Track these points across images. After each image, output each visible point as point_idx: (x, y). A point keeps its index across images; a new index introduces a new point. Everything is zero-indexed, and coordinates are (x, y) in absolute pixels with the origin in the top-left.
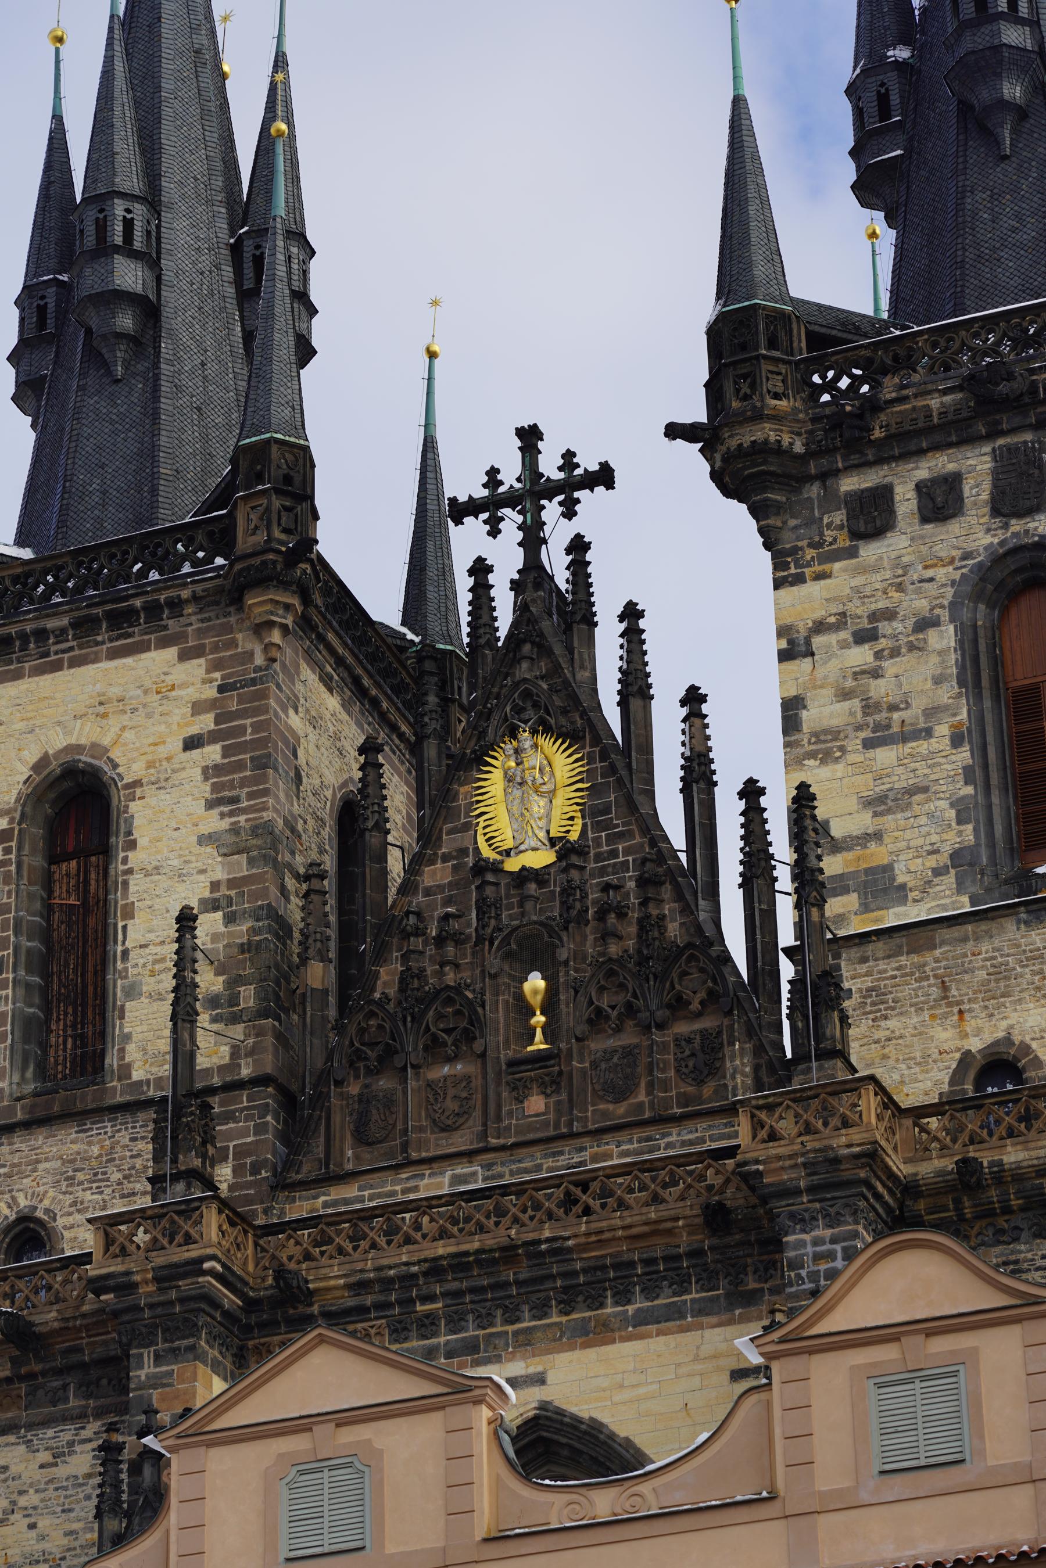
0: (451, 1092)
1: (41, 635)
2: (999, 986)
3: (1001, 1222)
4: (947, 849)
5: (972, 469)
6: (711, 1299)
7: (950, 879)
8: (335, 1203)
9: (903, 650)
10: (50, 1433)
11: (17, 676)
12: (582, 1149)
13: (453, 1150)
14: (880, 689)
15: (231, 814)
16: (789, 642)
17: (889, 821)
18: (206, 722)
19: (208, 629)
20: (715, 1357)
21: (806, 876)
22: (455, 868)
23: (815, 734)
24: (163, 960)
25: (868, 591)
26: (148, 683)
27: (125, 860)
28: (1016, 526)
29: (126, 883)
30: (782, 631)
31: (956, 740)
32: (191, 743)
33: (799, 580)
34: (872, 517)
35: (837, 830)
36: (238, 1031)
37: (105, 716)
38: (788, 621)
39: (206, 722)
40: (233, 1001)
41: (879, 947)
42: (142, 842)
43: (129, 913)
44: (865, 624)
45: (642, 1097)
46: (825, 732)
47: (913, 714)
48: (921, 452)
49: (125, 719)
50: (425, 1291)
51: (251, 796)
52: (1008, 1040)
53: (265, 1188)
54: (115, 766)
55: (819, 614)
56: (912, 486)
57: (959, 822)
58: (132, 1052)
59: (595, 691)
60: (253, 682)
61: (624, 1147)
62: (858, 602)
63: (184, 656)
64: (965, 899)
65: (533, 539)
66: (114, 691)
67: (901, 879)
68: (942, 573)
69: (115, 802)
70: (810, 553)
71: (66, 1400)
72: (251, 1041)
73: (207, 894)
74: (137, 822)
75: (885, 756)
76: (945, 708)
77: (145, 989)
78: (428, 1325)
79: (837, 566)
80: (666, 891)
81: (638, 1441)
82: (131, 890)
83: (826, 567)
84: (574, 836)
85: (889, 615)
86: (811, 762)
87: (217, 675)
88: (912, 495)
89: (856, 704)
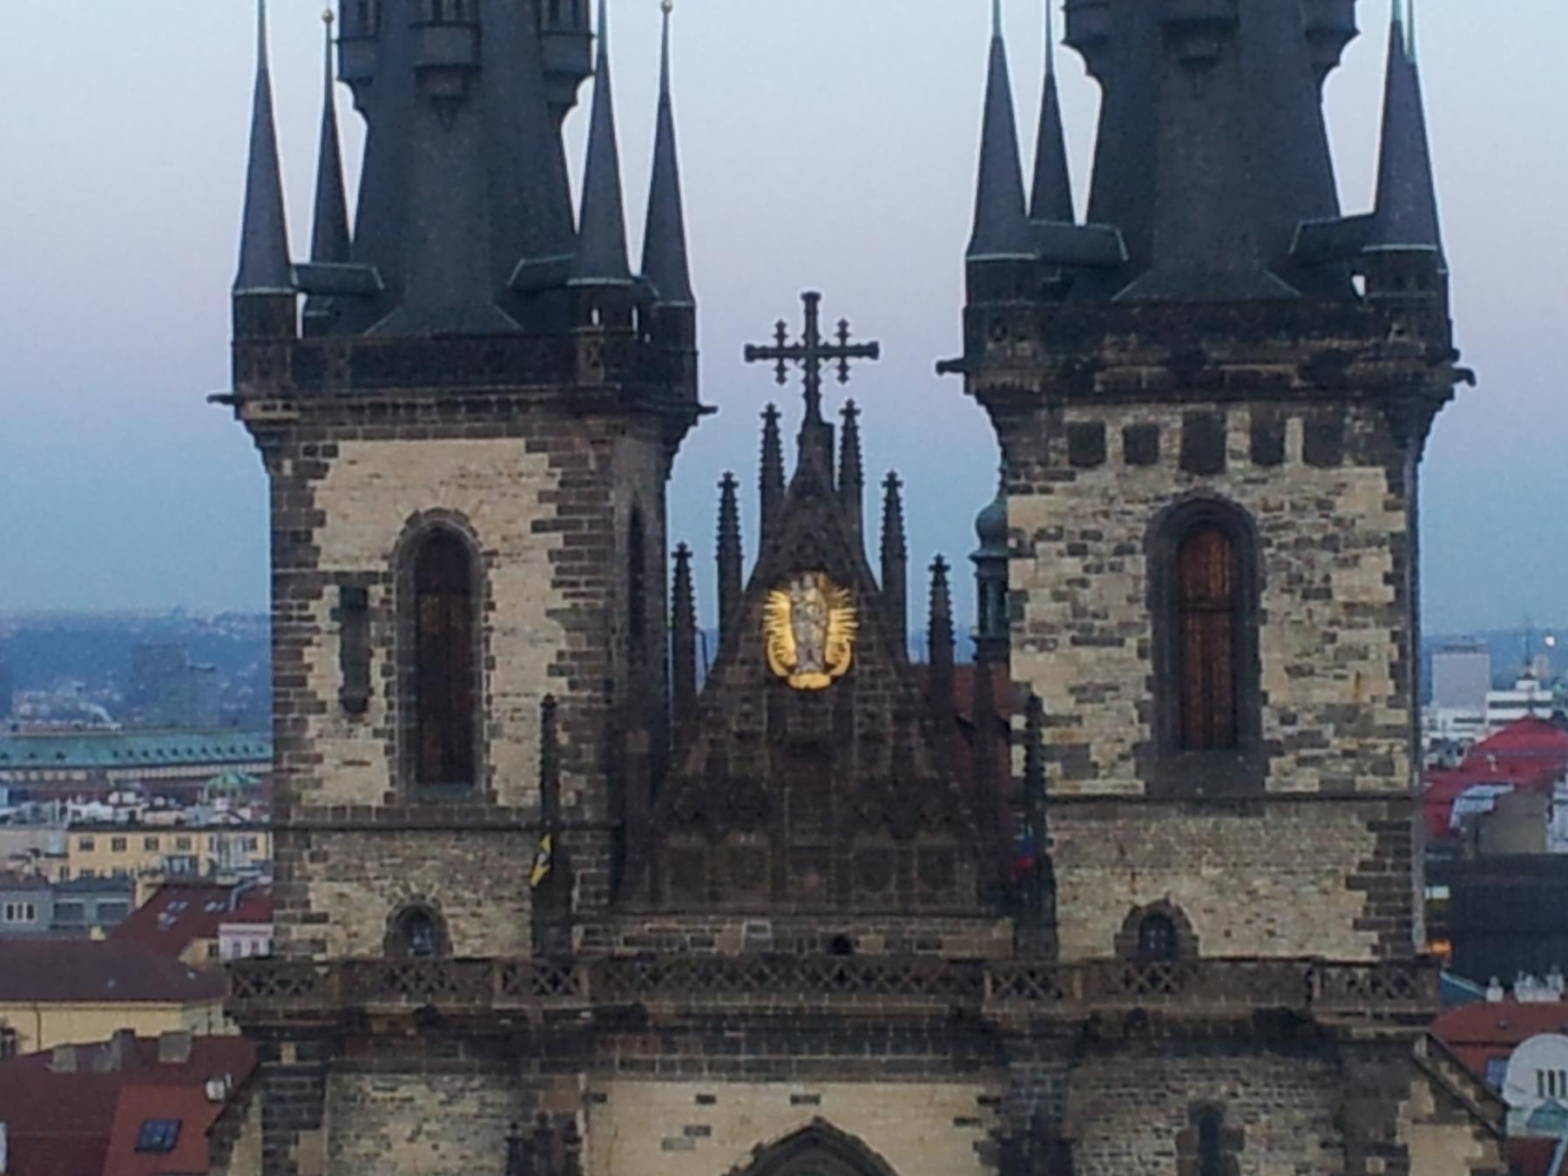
2: (1162, 860)
4: (1129, 741)
5: (1167, 425)
6: (944, 1062)
7: (1131, 765)
8: (658, 930)
9: (1106, 568)
12: (846, 923)
14: (1086, 596)
15: (573, 595)
17: (1088, 708)
18: (549, 511)
22: (752, 673)
24: (518, 710)
25: (1081, 512)
26: (501, 466)
27: (486, 619)
28: (1198, 481)
29: (487, 640)
31: (1142, 654)
32: (538, 527)
33: (1028, 491)
34: (1087, 449)
35: (1048, 709)
36: (581, 782)
39: (549, 511)
40: (578, 754)
41: (1076, 809)
42: (499, 605)
43: (491, 666)
44: (1078, 541)
45: (892, 889)
46: (1043, 624)
48: (1129, 402)
51: (588, 584)
52: (1166, 902)
54: (475, 534)
55: (1041, 524)
56: (1120, 428)
57: (1142, 720)
58: (497, 784)
60: (589, 483)
61: (880, 927)
62: (1071, 520)
63: (530, 448)
64: (1141, 784)
66: (472, 468)
67: (1094, 758)
70: (1038, 469)
71: (455, 1055)
72: (591, 792)
73: (554, 661)
74: (495, 587)
75: (1086, 654)
76: (1135, 624)
78: (734, 1046)
79: (1058, 485)
80: (914, 729)
81: (887, 1158)
82: (493, 644)
83: (1051, 484)
85: (1098, 536)
86: (1030, 648)
87: (558, 471)
88: (1119, 437)
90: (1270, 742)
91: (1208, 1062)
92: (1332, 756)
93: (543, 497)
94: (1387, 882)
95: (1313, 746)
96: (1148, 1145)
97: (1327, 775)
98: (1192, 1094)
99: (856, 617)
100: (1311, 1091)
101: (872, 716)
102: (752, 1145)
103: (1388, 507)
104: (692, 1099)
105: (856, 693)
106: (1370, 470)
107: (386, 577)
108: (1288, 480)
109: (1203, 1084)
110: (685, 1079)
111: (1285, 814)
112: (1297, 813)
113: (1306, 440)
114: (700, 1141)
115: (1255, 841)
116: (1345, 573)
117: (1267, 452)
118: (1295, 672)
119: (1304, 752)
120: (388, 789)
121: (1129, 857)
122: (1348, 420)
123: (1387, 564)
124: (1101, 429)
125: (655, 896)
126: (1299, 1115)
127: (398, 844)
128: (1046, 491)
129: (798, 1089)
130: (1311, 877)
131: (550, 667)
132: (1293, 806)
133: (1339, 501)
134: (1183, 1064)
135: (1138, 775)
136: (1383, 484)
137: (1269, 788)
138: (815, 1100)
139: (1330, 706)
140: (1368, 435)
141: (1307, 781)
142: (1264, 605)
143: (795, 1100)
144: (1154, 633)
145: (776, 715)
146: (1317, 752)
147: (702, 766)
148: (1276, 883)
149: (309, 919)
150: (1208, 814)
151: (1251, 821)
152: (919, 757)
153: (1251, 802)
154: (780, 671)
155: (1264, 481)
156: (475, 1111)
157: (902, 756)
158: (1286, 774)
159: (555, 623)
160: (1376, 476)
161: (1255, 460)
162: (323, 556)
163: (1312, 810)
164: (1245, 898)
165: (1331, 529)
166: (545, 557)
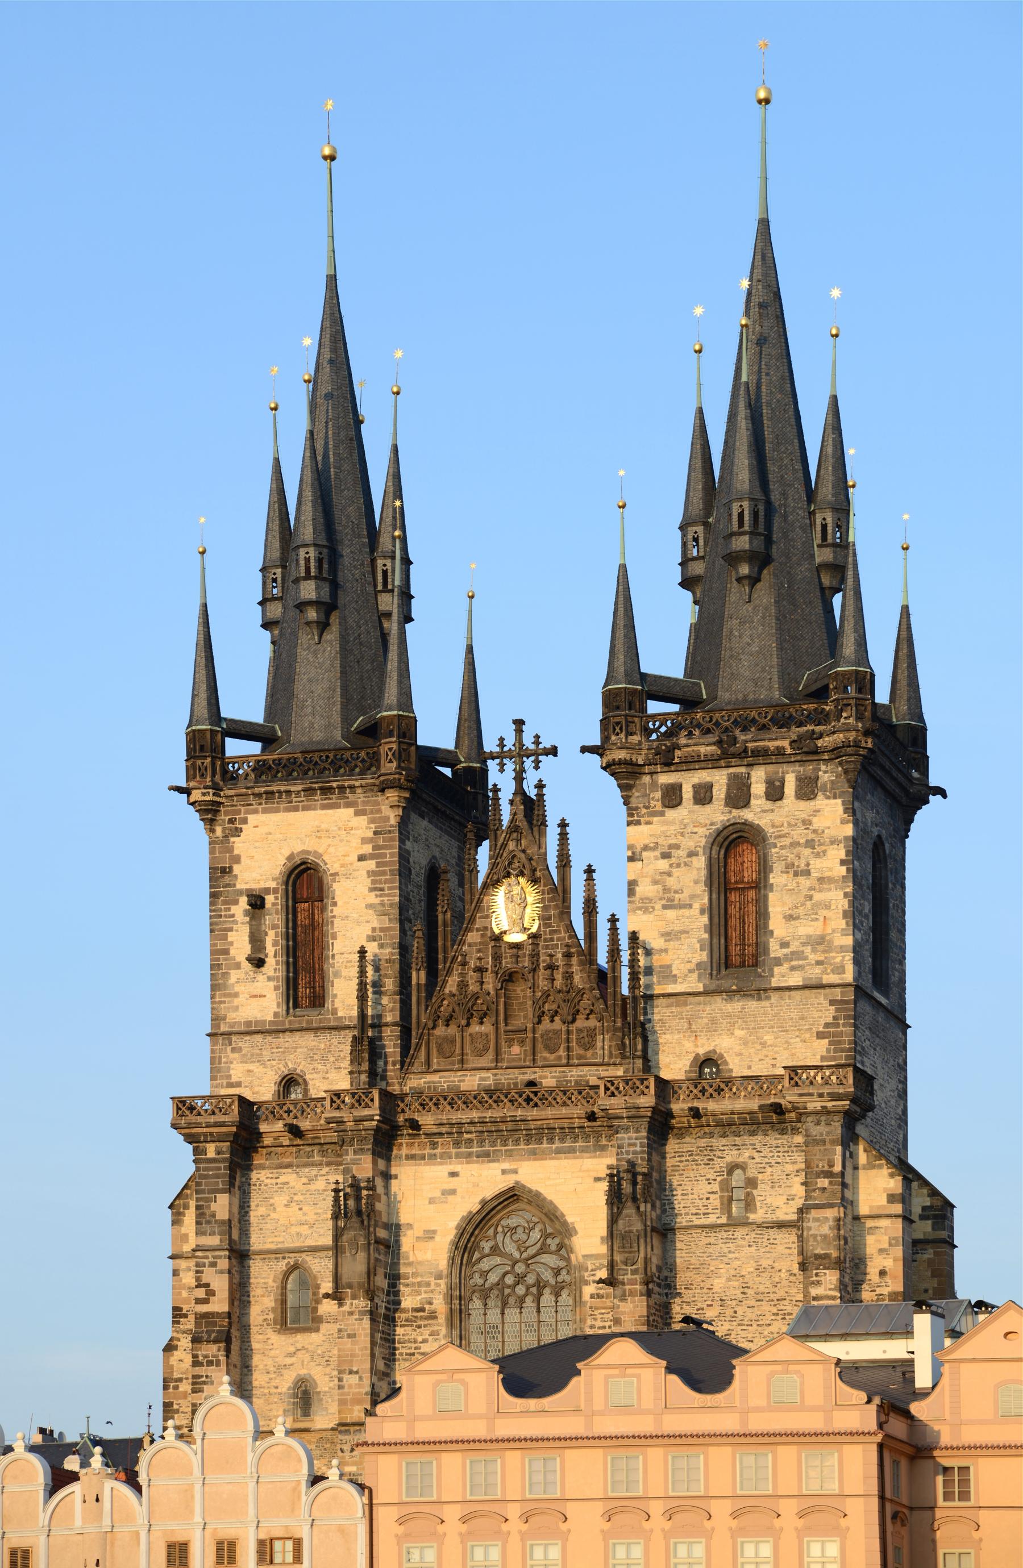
0: (479, 1040)
1: (288, 792)
2: (713, 1026)
3: (706, 1129)
4: (695, 961)
7: (695, 975)
8: (429, 1082)
10: (307, 1170)
11: (277, 810)
13: (480, 1065)
14: (671, 882)
15: (381, 896)
16: (633, 853)
18: (368, 849)
19: (368, 802)
20: (588, 1171)
21: (633, 962)
22: (482, 936)
23: (642, 899)
24: (351, 961)
27: (332, 911)
28: (735, 812)
29: (332, 922)
30: (630, 847)
31: (702, 912)
32: (361, 858)
33: (638, 823)
34: (672, 797)
37: (320, 837)
38: (633, 843)
43: (334, 937)
47: (684, 897)
49: (330, 841)
50: (468, 1130)
51: (390, 888)
52: (714, 1051)
53: (398, 1073)
54: (326, 864)
55: (646, 842)
59: (546, 859)
60: (390, 832)
62: (663, 838)
63: (357, 813)
65: (519, 778)
66: (324, 826)
68: (702, 831)
69: (325, 882)
70: (644, 811)
74: (337, 893)
75: (671, 914)
77: (343, 974)
79: (655, 819)
81: (556, 1202)
83: (650, 819)
84: (534, 930)
85: (677, 847)
86: (639, 912)
87: (373, 826)
88: (691, 790)
89: (660, 887)
90: (775, 958)
91: (738, 1140)
92: (809, 964)
93: (364, 841)
94: (841, 1033)
95: (799, 959)
96: (703, 1188)
97: (807, 975)
98: (729, 1159)
99: (542, 900)
100: (795, 1154)
101: (551, 956)
102: (480, 1198)
103: (843, 822)
104: (446, 1174)
105: (542, 944)
106: (832, 801)
107: (275, 891)
108: (786, 809)
109: (737, 1152)
110: (441, 1164)
111: (781, 998)
112: (790, 997)
113: (797, 786)
114: (450, 1198)
115: (765, 1014)
116: (818, 861)
117: (775, 793)
118: (789, 918)
119: (794, 963)
120: (277, 1010)
121: (693, 1026)
122: (820, 773)
123: (842, 854)
124: (681, 786)
125: (428, 1062)
126: (789, 1168)
127: (281, 1040)
128: (648, 823)
129: (506, 1166)
130: (797, 1033)
131: (368, 936)
132: (787, 993)
133: (815, 820)
134: (724, 1141)
135: (699, 980)
136: (840, 809)
137: (773, 985)
138: (515, 1172)
139: (809, 936)
140: (832, 782)
141: (795, 979)
142: (771, 881)
143: (504, 1172)
144: (710, 899)
145: (497, 958)
146: (801, 962)
147: (454, 990)
148: (776, 1038)
149: (231, 1085)
150: (738, 1001)
151: (764, 1003)
152: (577, 979)
153: (762, 992)
154: (497, 931)
155: (772, 811)
156: (323, 1187)
157: (568, 976)
158: (783, 976)
159: (371, 912)
160: (836, 804)
161: (767, 799)
162: (239, 881)
163: (797, 995)
164: (759, 1047)
165: (811, 836)
166: (365, 873)
